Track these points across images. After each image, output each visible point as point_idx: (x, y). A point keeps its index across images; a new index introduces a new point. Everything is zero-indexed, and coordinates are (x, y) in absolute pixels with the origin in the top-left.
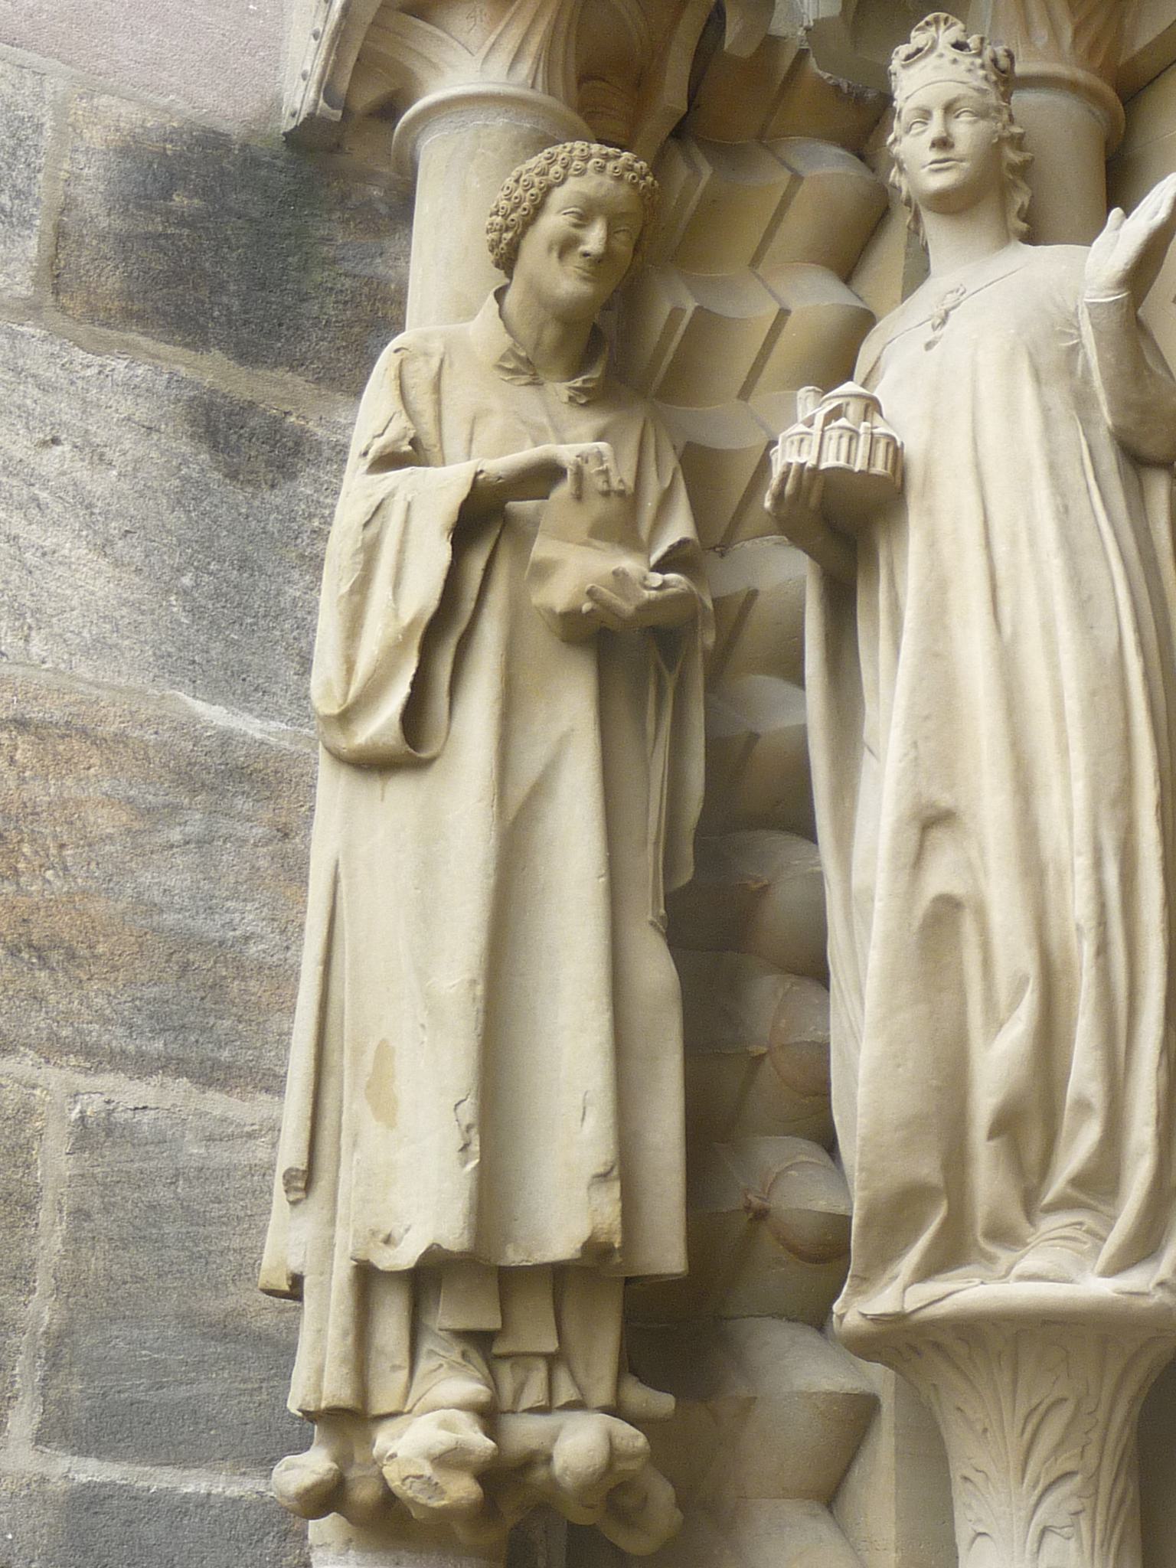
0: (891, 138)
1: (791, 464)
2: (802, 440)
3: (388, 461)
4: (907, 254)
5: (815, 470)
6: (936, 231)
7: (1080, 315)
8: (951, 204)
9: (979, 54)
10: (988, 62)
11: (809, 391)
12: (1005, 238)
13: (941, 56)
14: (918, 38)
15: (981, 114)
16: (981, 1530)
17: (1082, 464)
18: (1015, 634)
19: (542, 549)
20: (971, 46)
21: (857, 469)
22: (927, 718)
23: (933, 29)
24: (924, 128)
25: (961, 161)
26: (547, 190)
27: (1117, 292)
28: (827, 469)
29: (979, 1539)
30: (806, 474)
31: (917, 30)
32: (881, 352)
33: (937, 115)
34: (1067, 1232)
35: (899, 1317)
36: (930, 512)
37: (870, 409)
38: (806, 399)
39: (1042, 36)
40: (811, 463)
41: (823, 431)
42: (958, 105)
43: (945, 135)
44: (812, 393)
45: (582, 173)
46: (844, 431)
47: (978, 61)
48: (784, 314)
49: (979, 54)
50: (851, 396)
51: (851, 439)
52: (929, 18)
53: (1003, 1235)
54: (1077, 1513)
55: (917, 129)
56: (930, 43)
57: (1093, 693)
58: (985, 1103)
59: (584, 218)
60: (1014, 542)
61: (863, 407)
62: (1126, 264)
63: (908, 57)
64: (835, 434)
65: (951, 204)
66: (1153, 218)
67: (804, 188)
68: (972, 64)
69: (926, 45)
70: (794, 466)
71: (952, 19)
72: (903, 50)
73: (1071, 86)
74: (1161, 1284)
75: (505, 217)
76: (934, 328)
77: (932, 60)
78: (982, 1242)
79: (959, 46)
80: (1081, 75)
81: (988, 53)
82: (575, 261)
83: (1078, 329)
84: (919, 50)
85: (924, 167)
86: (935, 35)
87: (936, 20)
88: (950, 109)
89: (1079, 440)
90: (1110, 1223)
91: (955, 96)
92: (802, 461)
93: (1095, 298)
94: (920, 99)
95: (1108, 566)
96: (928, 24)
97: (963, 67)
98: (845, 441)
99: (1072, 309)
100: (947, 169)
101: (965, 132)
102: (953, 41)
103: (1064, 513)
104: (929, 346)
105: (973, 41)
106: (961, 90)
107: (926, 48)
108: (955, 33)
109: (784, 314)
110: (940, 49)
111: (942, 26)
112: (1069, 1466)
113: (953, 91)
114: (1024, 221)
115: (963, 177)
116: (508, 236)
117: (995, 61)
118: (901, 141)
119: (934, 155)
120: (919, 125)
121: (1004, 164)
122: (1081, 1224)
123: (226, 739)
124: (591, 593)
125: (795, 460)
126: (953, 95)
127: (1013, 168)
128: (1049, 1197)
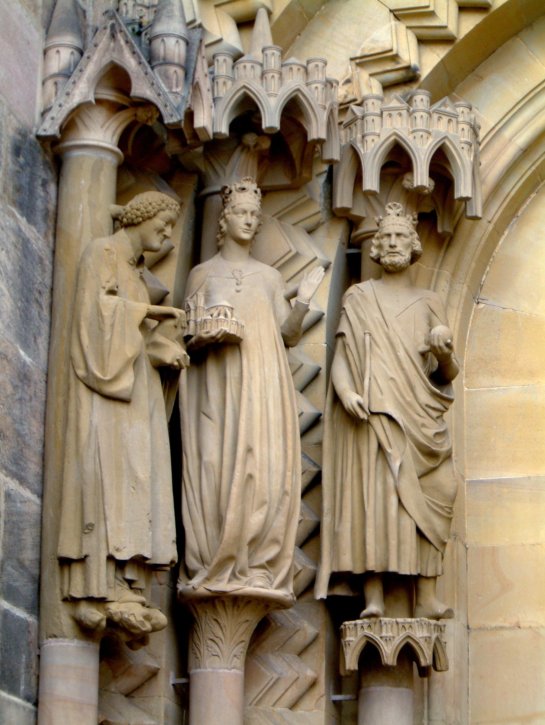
0: (226, 211)
1: (222, 329)
2: (224, 322)
3: (112, 292)
5: (228, 334)
8: (241, 242)
16: (214, 654)
19: (159, 338)
25: (252, 231)
26: (158, 211)
29: (213, 657)
33: (249, 214)
34: (262, 575)
35: (224, 592)
45: (171, 209)
53: (243, 573)
54: (241, 652)
58: (249, 535)
59: (167, 223)
65: (241, 242)
74: (292, 594)
75: (142, 213)
78: (237, 574)
79: (256, 192)
82: (161, 236)
84: (244, 189)
88: (252, 213)
90: (276, 576)
94: (245, 206)
96: (247, 180)
98: (236, 325)
104: (238, 291)
110: (250, 191)
112: (243, 639)
116: (141, 219)
122: (265, 573)
123: (24, 364)
124: (178, 361)
126: (255, 210)
128: (256, 564)
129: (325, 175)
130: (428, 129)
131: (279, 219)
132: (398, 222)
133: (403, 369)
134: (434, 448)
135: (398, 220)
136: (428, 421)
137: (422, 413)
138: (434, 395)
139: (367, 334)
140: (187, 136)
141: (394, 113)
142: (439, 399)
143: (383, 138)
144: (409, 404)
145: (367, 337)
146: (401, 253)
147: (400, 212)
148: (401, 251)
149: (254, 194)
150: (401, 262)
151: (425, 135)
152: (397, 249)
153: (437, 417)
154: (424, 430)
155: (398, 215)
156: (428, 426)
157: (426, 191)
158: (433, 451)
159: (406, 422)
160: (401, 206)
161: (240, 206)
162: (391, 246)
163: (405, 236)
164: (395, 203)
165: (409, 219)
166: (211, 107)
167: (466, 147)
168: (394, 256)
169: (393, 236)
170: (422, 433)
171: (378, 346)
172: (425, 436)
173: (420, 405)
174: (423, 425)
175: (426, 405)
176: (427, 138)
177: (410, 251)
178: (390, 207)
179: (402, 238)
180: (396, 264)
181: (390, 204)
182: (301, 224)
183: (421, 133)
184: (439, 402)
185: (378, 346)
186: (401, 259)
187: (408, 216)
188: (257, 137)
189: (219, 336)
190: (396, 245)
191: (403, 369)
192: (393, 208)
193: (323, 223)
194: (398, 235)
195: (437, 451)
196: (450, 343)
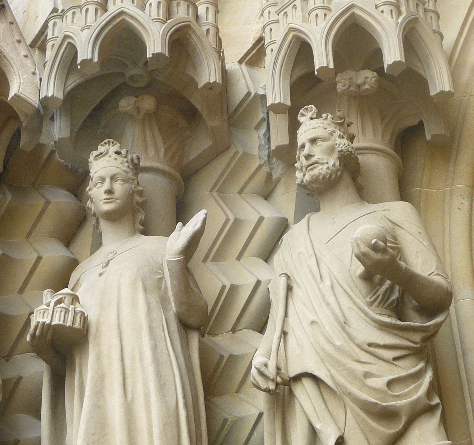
0: (88, 188)
1: (39, 322)
2: (44, 312)
4: (93, 236)
5: (49, 325)
6: (105, 227)
7: (164, 265)
9: (126, 157)
10: (129, 160)
11: (49, 291)
12: (134, 232)
13: (110, 156)
14: (101, 149)
15: (125, 181)
17: (163, 327)
18: (133, 399)
20: (123, 153)
21: (67, 325)
22: (93, 434)
23: (107, 145)
24: (102, 185)
25: (117, 199)
27: (179, 256)
28: (55, 325)
30: (45, 326)
31: (100, 146)
32: (80, 277)
33: (108, 180)
36: (98, 345)
37: (74, 300)
38: (47, 295)
39: (152, 151)
40: (48, 322)
41: (54, 309)
42: (116, 177)
43: (110, 188)
44: (50, 292)
46: (63, 309)
47: (125, 160)
48: (39, 258)
49: (126, 157)
50: (66, 294)
51: (65, 312)
52: (106, 141)
55: (99, 185)
56: (106, 151)
57: (165, 425)
60: (133, 359)
61: (71, 299)
62: (183, 245)
63: (97, 156)
64: (59, 310)
66: (194, 227)
67: (51, 207)
68: (123, 160)
69: (104, 151)
70: (40, 323)
71: (115, 142)
72: (95, 153)
73: (163, 173)
76: (103, 267)
77: (106, 157)
79: (118, 153)
80: (167, 168)
81: (129, 157)
83: (163, 271)
84: (101, 154)
85: (101, 201)
86: (108, 148)
87: (109, 142)
88: (113, 178)
89: (162, 316)
91: (115, 173)
92: (44, 321)
93: (170, 258)
94: (101, 173)
95: (173, 370)
96: (105, 143)
97: (119, 162)
98: (63, 313)
99: (161, 262)
100: (111, 202)
101: (118, 187)
102: (116, 151)
103: (155, 347)
104: (100, 275)
105: (124, 151)
106: (117, 171)
107: (104, 153)
108: (116, 148)
109: (39, 258)
111: (111, 145)
113: (114, 171)
114: (142, 225)
115: (117, 206)
117: (132, 160)
118: (92, 190)
119: (105, 196)
120: (100, 184)
121: (135, 201)
125: (41, 320)
127: (138, 204)
129: (265, 123)
130: (326, 5)
131: (220, 191)
132: (311, 126)
133: (328, 304)
134: (384, 404)
135: (310, 125)
136: (376, 367)
137: (365, 357)
138: (383, 327)
139: (282, 276)
140: (22, 120)
141: (289, 9)
142: (396, 332)
143: (279, 42)
144: (338, 349)
145: (283, 280)
146: (321, 161)
147: (313, 114)
148: (319, 159)
149: (116, 156)
150: (323, 172)
151: (321, 13)
152: (314, 159)
153: (395, 359)
154: (370, 382)
155: (312, 119)
156: (377, 373)
157: (367, 86)
158: (385, 408)
159: (339, 378)
160: (313, 106)
161: (97, 175)
162: (308, 157)
163: (324, 140)
164: (306, 107)
165: (326, 118)
166: (34, 73)
167: (387, 9)
168: (312, 169)
169: (308, 145)
170: (367, 386)
171: (299, 287)
172: (372, 389)
173: (358, 346)
174: (367, 375)
175: (370, 345)
176: (325, 15)
177: (336, 155)
178: (303, 115)
179: (319, 143)
180: (317, 177)
181: (301, 111)
182: (248, 189)
183: (314, 13)
184: (397, 335)
185: (299, 287)
186: (322, 169)
187: (324, 115)
188: (135, 99)
189: (38, 332)
190: (311, 154)
191: (328, 304)
192: (306, 114)
193: (279, 180)
194: (313, 141)
195: (391, 406)
196: (376, 243)
